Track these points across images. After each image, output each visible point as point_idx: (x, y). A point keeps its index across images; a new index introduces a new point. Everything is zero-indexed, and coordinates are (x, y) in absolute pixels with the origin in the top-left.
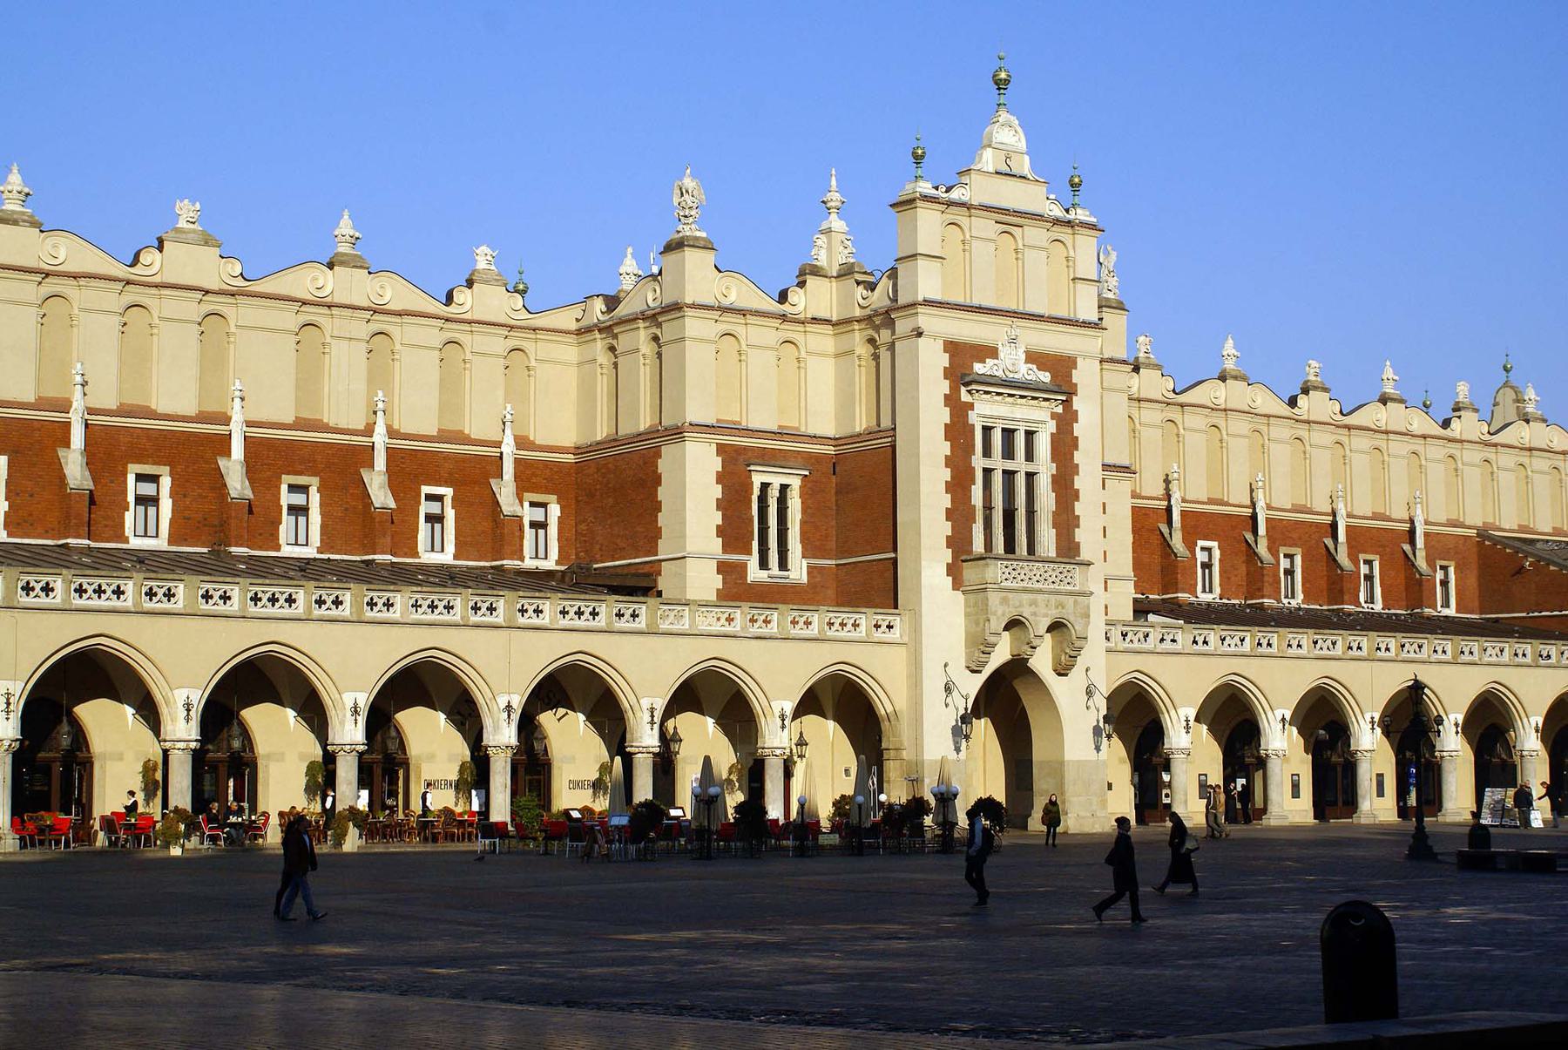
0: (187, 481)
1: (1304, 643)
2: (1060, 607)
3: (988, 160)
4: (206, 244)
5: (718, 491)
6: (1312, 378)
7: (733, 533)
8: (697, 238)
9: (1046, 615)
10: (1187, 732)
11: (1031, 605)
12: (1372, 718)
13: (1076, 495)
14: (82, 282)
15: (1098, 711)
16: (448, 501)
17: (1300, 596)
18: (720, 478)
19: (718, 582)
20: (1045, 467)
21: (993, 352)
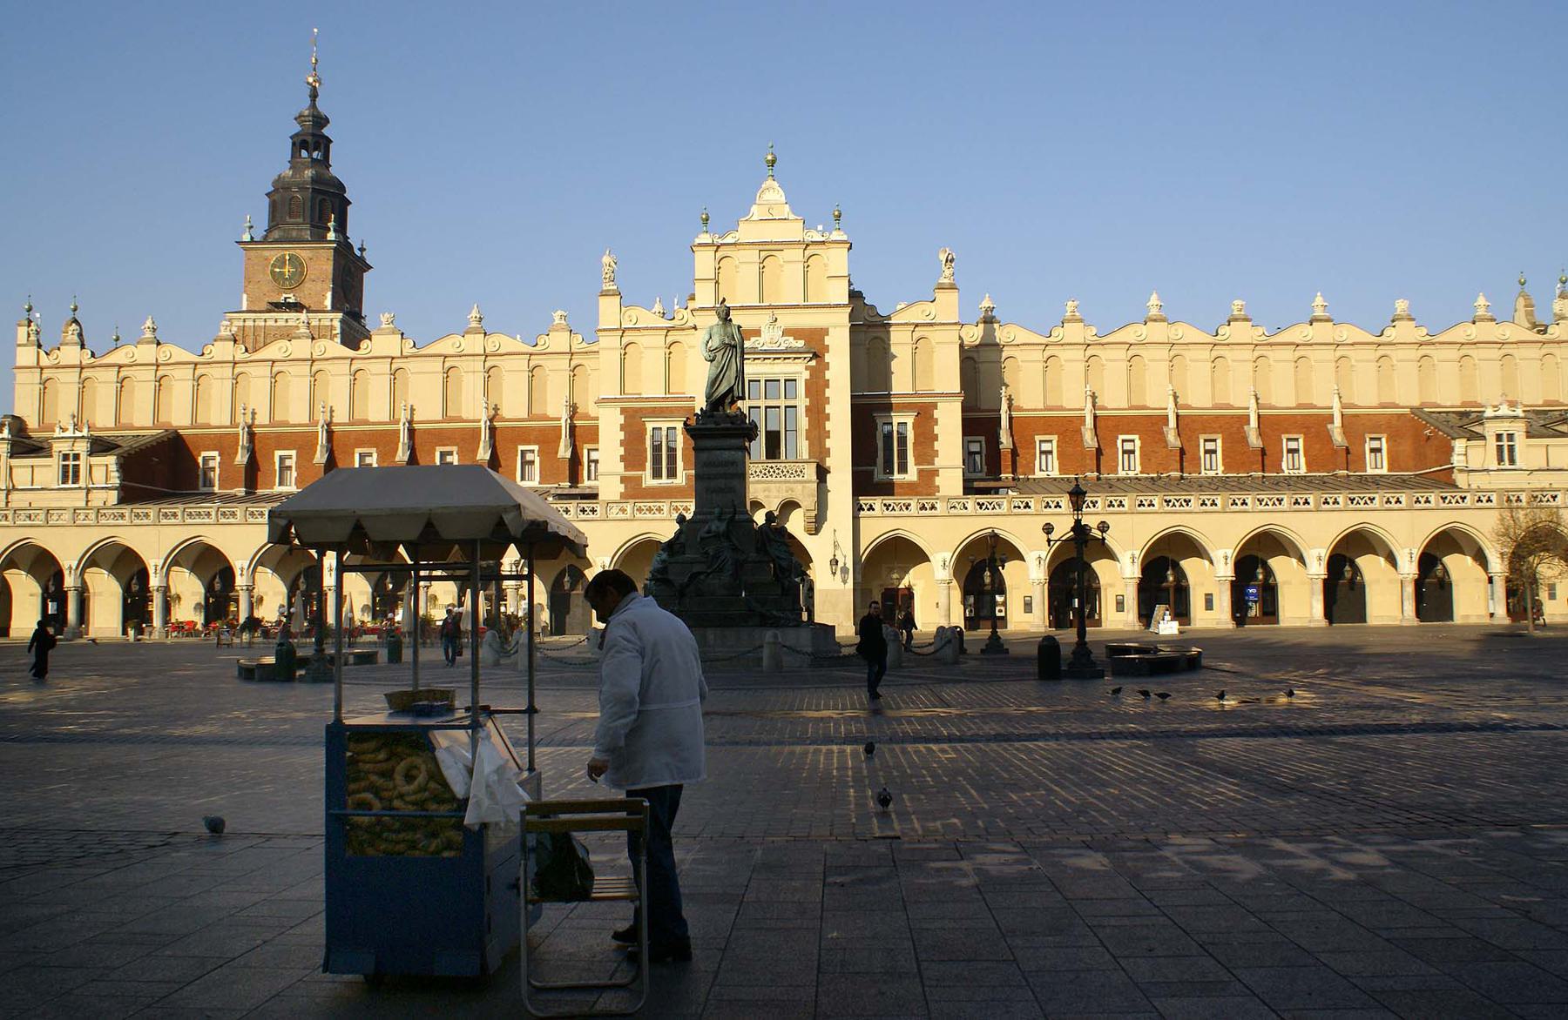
0: (385, 455)
1: (1340, 500)
2: (790, 492)
3: (756, 211)
4: (393, 333)
5: (621, 435)
6: (1236, 313)
7: (632, 458)
8: (609, 290)
9: (775, 497)
10: (944, 569)
11: (765, 491)
12: (1133, 555)
13: (827, 417)
14: (330, 362)
15: (845, 557)
16: (536, 452)
17: (1221, 468)
18: (622, 428)
19: (621, 488)
20: (802, 402)
21: (757, 333)
